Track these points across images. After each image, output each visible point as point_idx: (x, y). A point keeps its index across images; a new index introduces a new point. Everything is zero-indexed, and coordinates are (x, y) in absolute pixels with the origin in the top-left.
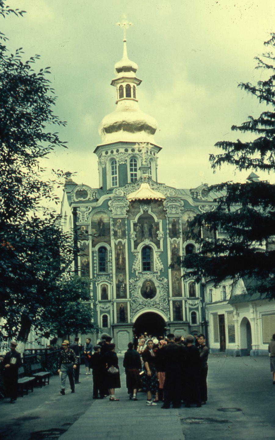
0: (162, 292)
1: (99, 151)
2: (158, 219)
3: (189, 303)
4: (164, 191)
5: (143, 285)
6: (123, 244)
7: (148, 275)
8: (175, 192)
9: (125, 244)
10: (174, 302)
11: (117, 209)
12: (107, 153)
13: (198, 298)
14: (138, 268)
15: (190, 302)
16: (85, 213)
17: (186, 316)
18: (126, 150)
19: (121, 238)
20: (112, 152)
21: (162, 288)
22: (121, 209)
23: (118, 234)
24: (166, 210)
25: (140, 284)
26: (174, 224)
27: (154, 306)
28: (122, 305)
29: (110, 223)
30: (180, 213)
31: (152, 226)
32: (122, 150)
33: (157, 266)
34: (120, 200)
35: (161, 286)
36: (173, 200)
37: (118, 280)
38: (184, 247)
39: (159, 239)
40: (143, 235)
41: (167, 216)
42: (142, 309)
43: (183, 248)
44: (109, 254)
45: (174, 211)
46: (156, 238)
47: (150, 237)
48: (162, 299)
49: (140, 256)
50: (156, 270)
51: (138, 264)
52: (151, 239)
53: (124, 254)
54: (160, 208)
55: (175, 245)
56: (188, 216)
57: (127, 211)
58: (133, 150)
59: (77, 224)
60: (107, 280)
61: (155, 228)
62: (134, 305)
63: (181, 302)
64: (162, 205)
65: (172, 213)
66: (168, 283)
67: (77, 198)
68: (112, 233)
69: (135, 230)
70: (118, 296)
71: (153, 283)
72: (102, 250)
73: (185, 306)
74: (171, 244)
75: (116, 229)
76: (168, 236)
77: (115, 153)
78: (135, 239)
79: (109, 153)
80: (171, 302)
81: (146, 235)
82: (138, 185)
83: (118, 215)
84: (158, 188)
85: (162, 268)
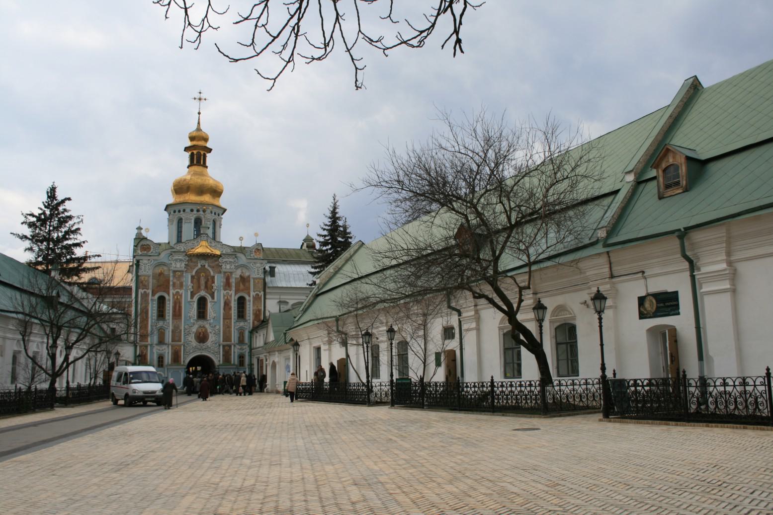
1: (169, 209)
5: (197, 330)
7: (201, 323)
10: (224, 346)
12: (175, 212)
13: (247, 344)
15: (238, 347)
17: (234, 359)
18: (192, 210)
20: (179, 211)
21: (214, 334)
25: (194, 329)
26: (228, 279)
31: (208, 279)
32: (188, 210)
38: (236, 298)
39: (213, 290)
40: (199, 287)
43: (235, 300)
44: (167, 303)
45: (228, 267)
46: (211, 290)
49: (195, 305)
54: (217, 263)
58: (198, 211)
63: (230, 346)
65: (227, 267)
67: (141, 252)
68: (171, 283)
70: (172, 341)
71: (206, 330)
72: (162, 300)
74: (224, 296)
75: (175, 281)
76: (222, 288)
77: (182, 210)
78: (192, 290)
79: (177, 211)
80: (221, 347)
81: (203, 287)
82: (197, 242)
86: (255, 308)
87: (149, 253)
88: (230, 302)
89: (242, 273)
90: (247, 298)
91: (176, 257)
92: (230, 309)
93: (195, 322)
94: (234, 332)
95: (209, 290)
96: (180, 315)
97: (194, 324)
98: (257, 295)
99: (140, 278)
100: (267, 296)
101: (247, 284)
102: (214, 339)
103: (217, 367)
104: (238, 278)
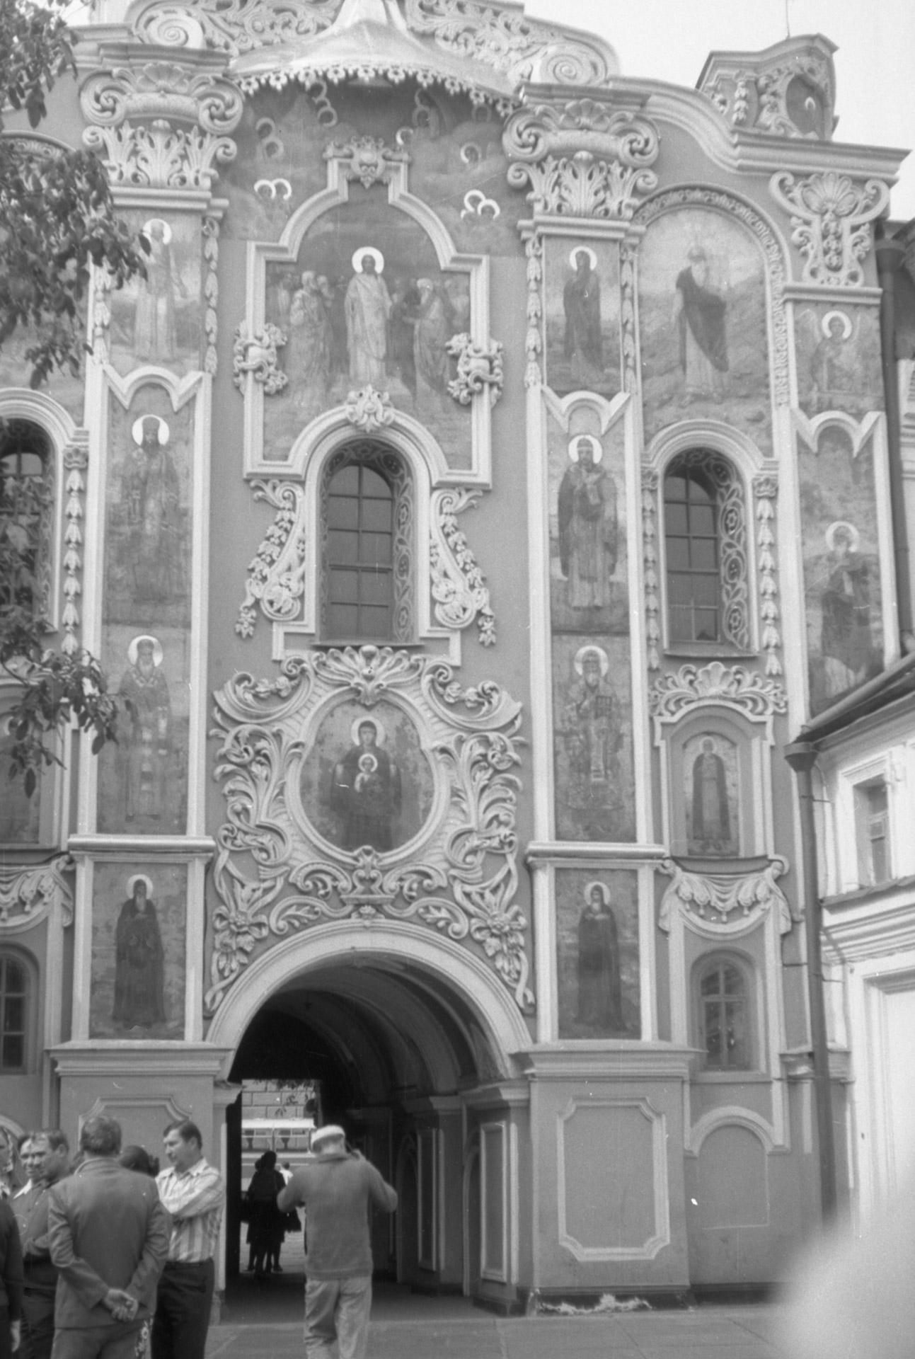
0: (471, 797)
2: (458, 250)
3: (686, 891)
4: (514, 56)
6: (176, 405)
8: (595, 67)
9: (190, 403)
11: (144, 145)
13: (764, 861)
14: (285, 598)
19: (167, 363)
22: (176, 147)
23: (143, 326)
24: (523, 179)
25: (299, 724)
26: (580, 295)
27: (412, 909)
28: (140, 885)
30: (629, 213)
31: (413, 297)
33: (437, 596)
34: (170, 72)
35: (472, 749)
36: (579, 110)
38: (659, 467)
41: (532, 229)
42: (305, 926)
43: (646, 475)
45: (581, 194)
46: (439, 385)
47: (390, 374)
48: (474, 852)
50: (434, 621)
51: (291, 573)
55: (585, 444)
57: (217, 163)
61: (435, 311)
62: (243, 894)
64: (503, 152)
66: (527, 728)
69: (273, 315)
71: (405, 734)
73: (657, 916)
74: (557, 439)
76: (534, 374)
80: (544, 882)
83: (149, 185)
84: (469, 30)
85: (480, 614)
90: (749, 465)
91: (139, 98)
92: (614, 545)
93: (310, 658)
94: (655, 750)
97: (298, 676)
98: (834, 435)
102: (475, 813)
103: (507, 1068)
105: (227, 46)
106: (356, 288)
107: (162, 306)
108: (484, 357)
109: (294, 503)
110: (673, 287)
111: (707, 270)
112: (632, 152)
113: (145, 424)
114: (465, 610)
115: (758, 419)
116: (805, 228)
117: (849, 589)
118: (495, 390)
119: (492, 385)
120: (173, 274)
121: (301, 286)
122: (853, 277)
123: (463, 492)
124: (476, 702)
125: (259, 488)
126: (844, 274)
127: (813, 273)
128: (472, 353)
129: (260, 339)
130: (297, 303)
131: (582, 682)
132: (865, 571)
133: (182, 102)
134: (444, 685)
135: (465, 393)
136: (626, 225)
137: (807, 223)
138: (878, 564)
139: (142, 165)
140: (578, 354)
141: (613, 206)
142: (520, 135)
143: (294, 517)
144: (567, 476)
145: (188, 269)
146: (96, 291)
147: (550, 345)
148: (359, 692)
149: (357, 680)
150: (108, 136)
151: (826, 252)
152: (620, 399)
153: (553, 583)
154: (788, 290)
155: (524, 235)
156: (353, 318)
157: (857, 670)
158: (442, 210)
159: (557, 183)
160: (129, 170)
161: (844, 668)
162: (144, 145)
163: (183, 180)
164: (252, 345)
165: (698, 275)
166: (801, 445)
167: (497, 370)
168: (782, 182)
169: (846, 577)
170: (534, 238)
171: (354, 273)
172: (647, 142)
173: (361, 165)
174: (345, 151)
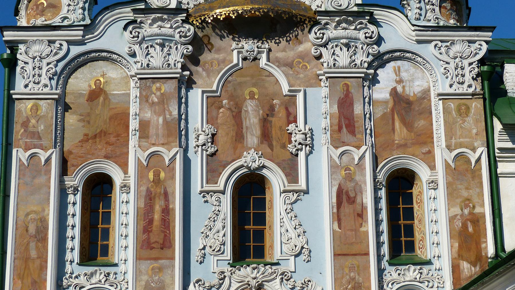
11: (151, 50)
16: (45, 62)
19: (163, 144)
29: (129, 95)
30: (366, 65)
31: (272, 108)
37: (143, 283)
40: (239, 137)
46: (284, 147)
47: (262, 143)
52: (269, 150)
53: (170, 198)
56: (394, 76)
59: (14, 96)
60: (107, 286)
61: (281, 114)
68: (134, 124)
75: (148, 115)
81: (253, 138)
85: (303, 248)
86: (457, 210)
87: (56, 21)
88: (359, 190)
89: (400, 81)
92: (361, 215)
95: (277, 149)
96: (167, 244)
99: (18, 106)
100: (502, 168)
101: (421, 123)
104: (386, 102)
105: (188, 4)
106: (247, 105)
107: (161, 120)
108: (303, 134)
109: (220, 202)
110: (387, 96)
111: (404, 87)
112: (366, 38)
113: (154, 172)
114: (296, 246)
115: (429, 152)
116: (447, 66)
117: (470, 229)
118: (308, 148)
119: (306, 146)
120: (166, 106)
121: (222, 107)
122: (470, 86)
123: (295, 194)
124: (301, 287)
125: (204, 197)
126: (465, 85)
127: (451, 86)
128: (297, 132)
129: (204, 132)
130: (221, 115)
131: (348, 277)
132: (478, 221)
133: (167, 29)
134: (287, 280)
135: (294, 150)
136: (365, 70)
137: (448, 63)
138: (484, 216)
139: (151, 59)
140: (344, 129)
141: (358, 62)
142: (316, 33)
143: (220, 208)
144: (339, 185)
145: (172, 103)
146: (132, 116)
147: (331, 126)
148: (249, 285)
149: (249, 279)
150: (136, 48)
151: (457, 76)
152: (364, 148)
153: (334, 232)
154: (439, 95)
155: (320, 77)
156: (246, 119)
157: (475, 266)
158: (284, 68)
159: (334, 54)
160: (145, 62)
161: (469, 265)
162: (151, 50)
163: (169, 65)
164: (201, 134)
165: (399, 89)
166: (447, 165)
167: (308, 139)
168: (436, 46)
169: (469, 224)
170: (324, 78)
171: (245, 99)
172: (373, 32)
173: (247, 51)
174: (240, 46)
